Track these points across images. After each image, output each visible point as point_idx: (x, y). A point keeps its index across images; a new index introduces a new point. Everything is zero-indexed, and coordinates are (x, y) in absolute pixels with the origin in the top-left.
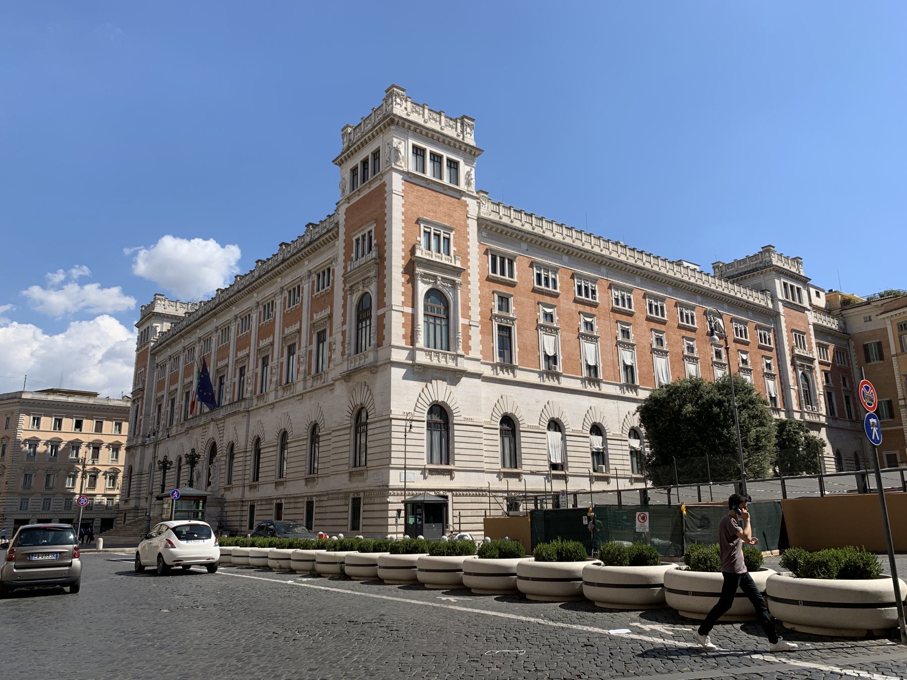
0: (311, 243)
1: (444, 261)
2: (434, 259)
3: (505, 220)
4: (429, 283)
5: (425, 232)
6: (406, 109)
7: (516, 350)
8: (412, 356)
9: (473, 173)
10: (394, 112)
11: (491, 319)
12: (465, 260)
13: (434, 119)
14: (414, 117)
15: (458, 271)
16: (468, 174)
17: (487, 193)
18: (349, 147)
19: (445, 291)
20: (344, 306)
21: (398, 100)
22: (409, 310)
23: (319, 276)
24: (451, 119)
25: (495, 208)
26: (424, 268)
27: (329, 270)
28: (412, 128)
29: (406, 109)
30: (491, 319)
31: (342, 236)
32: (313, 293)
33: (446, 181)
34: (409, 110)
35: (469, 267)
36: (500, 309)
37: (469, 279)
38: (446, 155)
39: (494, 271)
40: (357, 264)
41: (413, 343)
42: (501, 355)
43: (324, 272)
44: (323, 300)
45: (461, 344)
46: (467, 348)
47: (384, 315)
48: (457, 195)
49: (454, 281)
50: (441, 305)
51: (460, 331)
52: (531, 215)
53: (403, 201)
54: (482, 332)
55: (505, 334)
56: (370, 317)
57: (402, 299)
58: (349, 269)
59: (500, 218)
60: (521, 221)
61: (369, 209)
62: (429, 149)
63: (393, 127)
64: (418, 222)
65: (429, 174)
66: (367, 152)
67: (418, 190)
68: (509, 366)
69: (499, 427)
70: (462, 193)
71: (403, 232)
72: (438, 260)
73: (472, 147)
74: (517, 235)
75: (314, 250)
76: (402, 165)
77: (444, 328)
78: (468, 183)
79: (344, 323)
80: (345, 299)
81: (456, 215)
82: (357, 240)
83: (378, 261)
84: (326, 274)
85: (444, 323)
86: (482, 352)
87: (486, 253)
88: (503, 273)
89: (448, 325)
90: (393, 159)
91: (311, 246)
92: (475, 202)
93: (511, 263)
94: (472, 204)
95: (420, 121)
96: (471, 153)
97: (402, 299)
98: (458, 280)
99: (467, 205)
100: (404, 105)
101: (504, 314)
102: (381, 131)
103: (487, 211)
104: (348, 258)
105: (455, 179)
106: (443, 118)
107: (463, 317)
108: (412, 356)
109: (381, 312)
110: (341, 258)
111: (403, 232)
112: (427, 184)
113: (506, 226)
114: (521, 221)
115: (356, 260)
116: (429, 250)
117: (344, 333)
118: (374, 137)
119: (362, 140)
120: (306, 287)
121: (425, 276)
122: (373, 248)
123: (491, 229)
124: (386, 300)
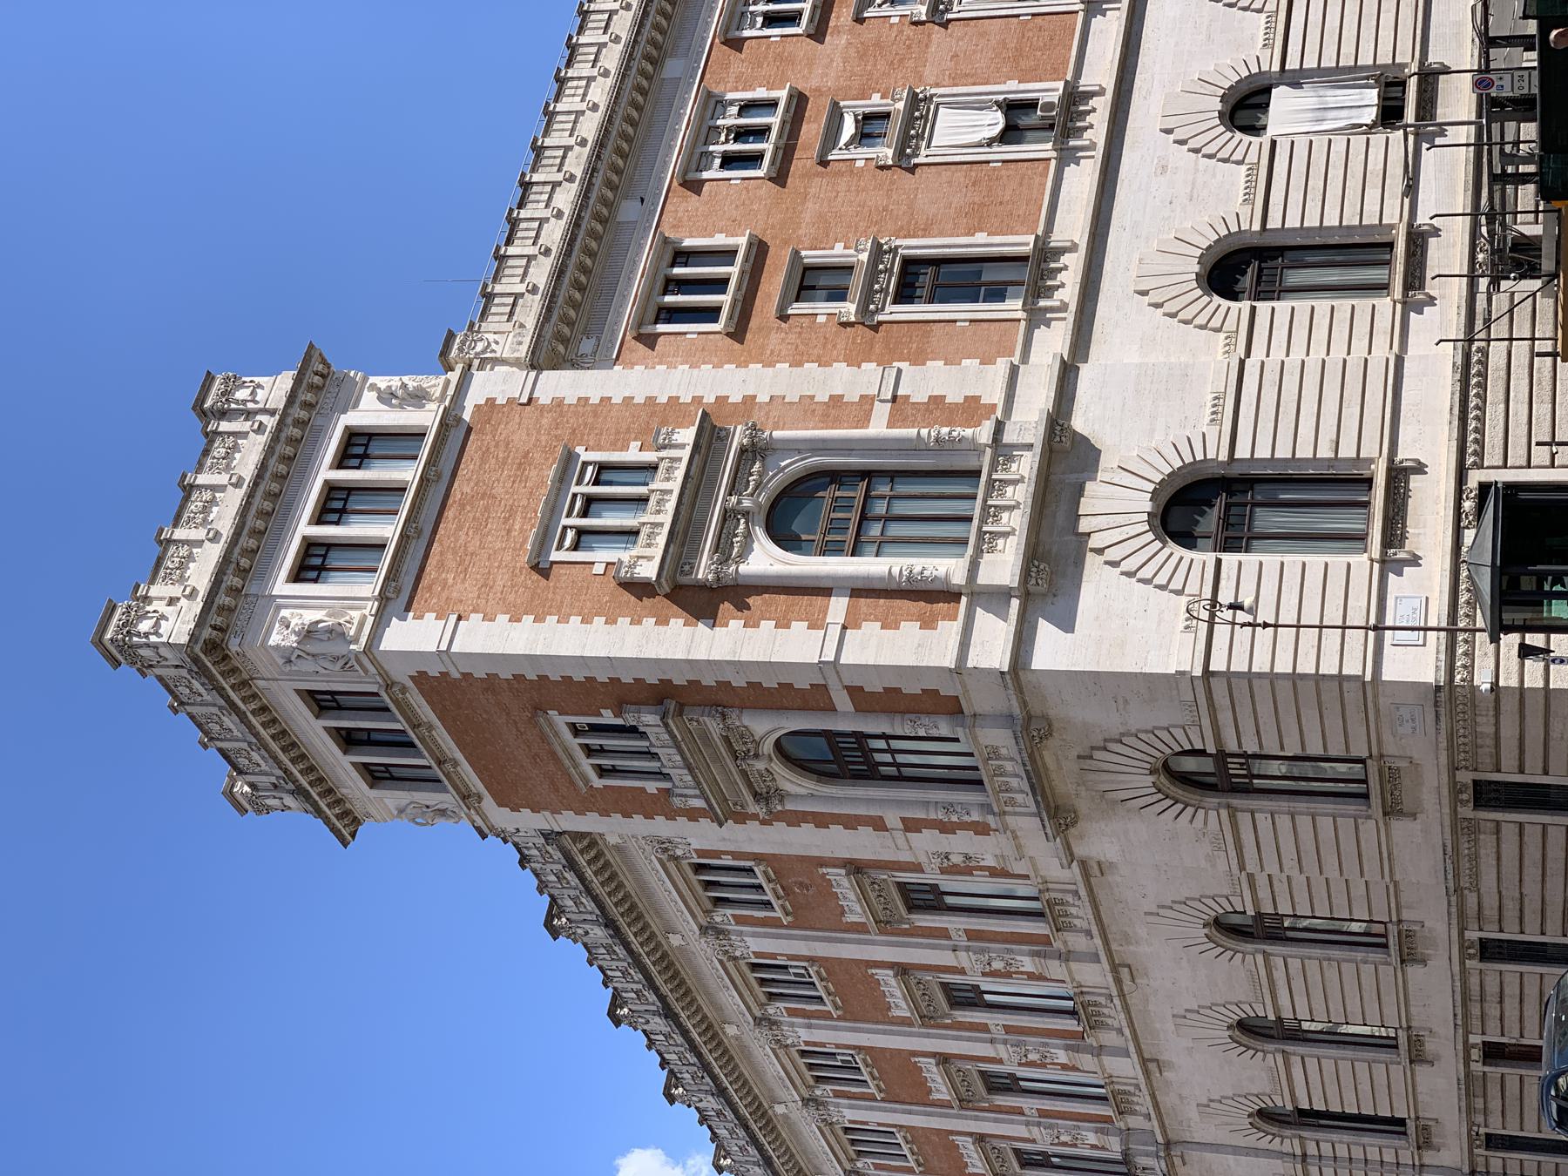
0: (610, 924)
1: (675, 485)
2: (667, 518)
3: (541, 274)
4: (748, 536)
5: (576, 547)
6: (172, 601)
7: (981, 242)
8: (995, 598)
9: (382, 382)
10: (184, 639)
11: (875, 328)
12: (673, 410)
13: (205, 510)
14: (201, 574)
15: (710, 437)
16: (387, 397)
17: (451, 336)
18: (299, 792)
19: (775, 483)
20: (821, 821)
21: (144, 626)
22: (838, 607)
23: (719, 901)
24: (206, 452)
25: (500, 307)
26: (696, 552)
27: (699, 868)
28: (237, 582)
29: (172, 601)
30: (875, 328)
31: (589, 823)
32: (776, 923)
33: (408, 473)
34: (176, 591)
35: (697, 400)
36: (839, 294)
37: (735, 398)
38: (325, 473)
39: (711, 313)
40: (681, 775)
41: (952, 596)
42: (997, 293)
43: (709, 885)
44: (801, 891)
45: (959, 432)
46: (972, 409)
47: (855, 692)
48: (456, 437)
49: (743, 451)
50: (825, 498)
51: (911, 432)
52: (526, 186)
53: (476, 618)
54: (918, 359)
55: (926, 278)
56: (861, 737)
57: (799, 627)
58: (699, 803)
59: (534, 290)
60: (543, 221)
61: (499, 732)
62: (304, 528)
63: (233, 646)
64: (542, 569)
65: (387, 530)
66: (314, 732)
67: (441, 565)
68: (1035, 270)
69: (1245, 305)
70: (449, 421)
71: (575, 620)
72: (671, 506)
73: (298, 381)
74: (592, 234)
75: (634, 913)
76: (358, 618)
78: (418, 398)
79: (879, 825)
80: (795, 819)
81: (520, 439)
82: (602, 772)
83: (672, 705)
84: (713, 881)
85: (883, 489)
86: (987, 361)
87: (650, 341)
88: (719, 284)
89: (893, 475)
90: (336, 648)
91: (622, 923)
92: (478, 377)
93: (684, 256)
94: (487, 386)
95: (211, 555)
96: (318, 386)
97: (799, 627)
98: (739, 438)
99: (491, 402)
100: (159, 606)
101: (857, 283)
102: (245, 684)
103: (509, 335)
104: (661, 806)
105: (402, 441)
106: (202, 479)
107: (864, 421)
108: (995, 598)
109: (842, 701)
110: (661, 827)
111: (575, 620)
112: (420, 535)
113: (559, 273)
114: (543, 221)
115: (667, 777)
116: (637, 533)
117: (911, 826)
118: (264, 709)
119: (274, 746)
120: (756, 944)
121: (722, 547)
122: (630, 720)
123: (571, 324)
124: (802, 683)
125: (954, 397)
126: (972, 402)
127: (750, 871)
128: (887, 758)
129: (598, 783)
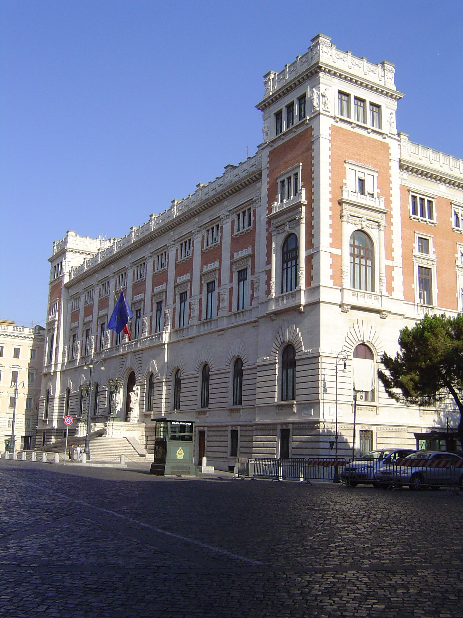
46: (390, 289)
54: (404, 274)
77: (369, 269)
80: (269, 240)
125: (394, 284)
126: (393, 289)
127: (249, 225)
128: (289, 265)
129: (278, 181)
